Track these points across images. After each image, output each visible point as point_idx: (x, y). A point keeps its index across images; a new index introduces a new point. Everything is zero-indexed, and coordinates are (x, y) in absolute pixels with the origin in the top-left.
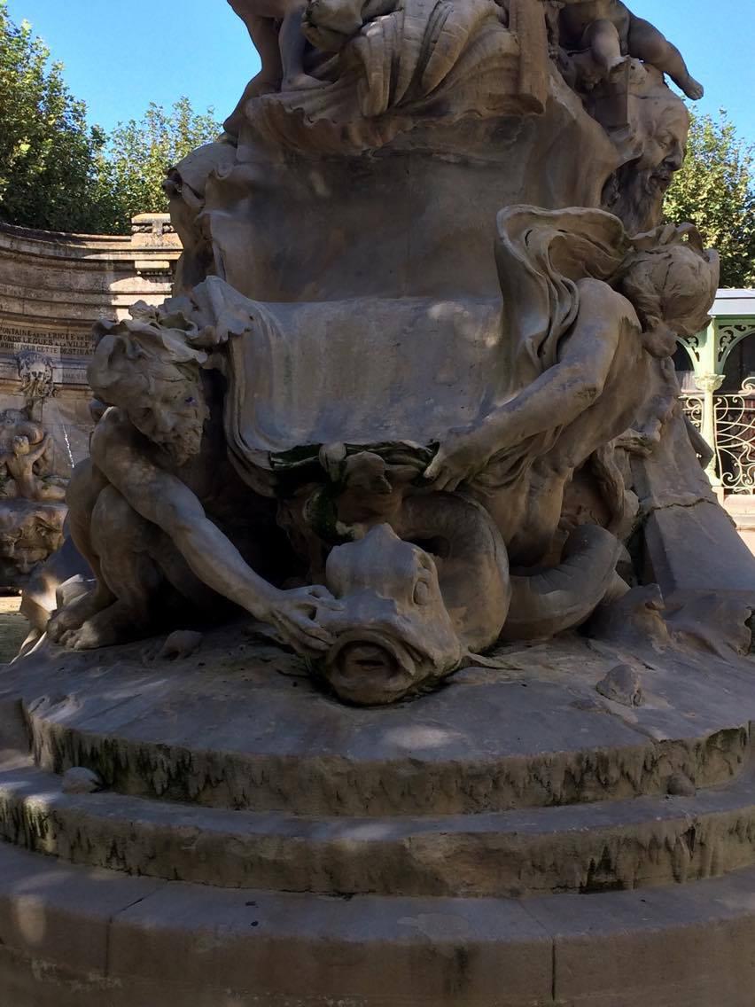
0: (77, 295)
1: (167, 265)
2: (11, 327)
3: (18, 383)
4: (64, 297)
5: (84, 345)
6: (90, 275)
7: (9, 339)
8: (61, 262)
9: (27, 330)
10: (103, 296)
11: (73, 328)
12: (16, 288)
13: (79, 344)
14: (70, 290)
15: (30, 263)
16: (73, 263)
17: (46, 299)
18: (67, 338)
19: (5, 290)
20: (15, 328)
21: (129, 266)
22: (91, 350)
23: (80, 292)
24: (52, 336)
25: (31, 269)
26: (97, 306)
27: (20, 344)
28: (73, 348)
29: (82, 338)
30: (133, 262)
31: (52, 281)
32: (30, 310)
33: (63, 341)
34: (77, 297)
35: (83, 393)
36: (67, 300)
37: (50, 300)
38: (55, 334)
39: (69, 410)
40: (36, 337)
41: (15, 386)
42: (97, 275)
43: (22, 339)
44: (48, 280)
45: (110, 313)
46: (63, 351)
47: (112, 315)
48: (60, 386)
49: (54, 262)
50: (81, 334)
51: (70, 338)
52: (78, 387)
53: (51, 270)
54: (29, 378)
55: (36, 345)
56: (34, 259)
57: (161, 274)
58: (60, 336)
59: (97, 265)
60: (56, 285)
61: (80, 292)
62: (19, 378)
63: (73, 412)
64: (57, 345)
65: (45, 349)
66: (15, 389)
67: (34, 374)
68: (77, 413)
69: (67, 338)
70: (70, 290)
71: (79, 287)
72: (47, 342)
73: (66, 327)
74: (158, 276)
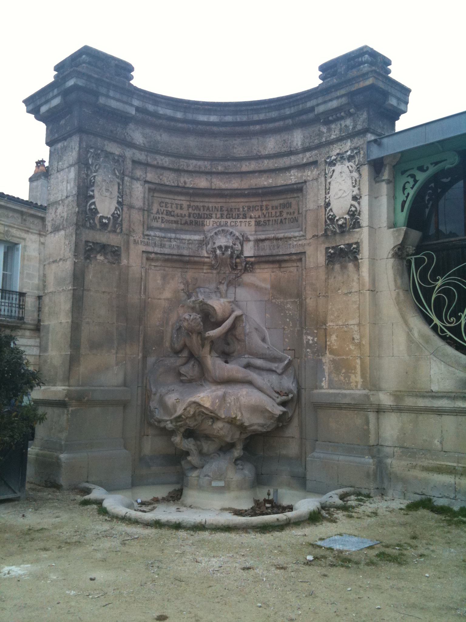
0: (266, 161)
1: (344, 100)
2: (201, 204)
3: (206, 260)
4: (253, 166)
5: (278, 214)
6: (278, 137)
7: (200, 216)
8: (245, 128)
9: (220, 205)
10: (293, 158)
11: (268, 198)
12: (200, 163)
13: (274, 213)
14: (259, 158)
15: (214, 135)
16: (258, 127)
17: (234, 170)
18: (262, 210)
19: (188, 166)
20: (206, 205)
21: (311, 116)
22: (285, 219)
23: (269, 157)
24: (246, 209)
25: (218, 142)
26: (288, 169)
27: (212, 220)
28: (267, 219)
29: (277, 208)
30: (312, 109)
31: (239, 151)
32: (219, 183)
33: (259, 213)
34: (267, 164)
35: (277, 266)
36: (257, 169)
37: (239, 171)
38: (249, 208)
39: (263, 285)
40: (230, 213)
41: (204, 263)
42: (285, 136)
43: (214, 216)
44: (235, 151)
45: (300, 175)
46: (258, 224)
47: (302, 176)
48: (253, 259)
49: (238, 129)
50: (276, 203)
51: (264, 208)
52: (271, 259)
53: (238, 141)
54: (215, 252)
55: (229, 221)
56: (215, 129)
57: (343, 114)
58: (254, 208)
59: (281, 123)
60: (243, 154)
61: (269, 157)
62: (206, 255)
63: (268, 286)
64: (251, 218)
65: (239, 224)
66: (205, 267)
67: (220, 247)
68: (273, 287)
69: (262, 210)
70: (259, 158)
71: (267, 153)
72: (241, 216)
73: (260, 199)
74: (342, 118)
